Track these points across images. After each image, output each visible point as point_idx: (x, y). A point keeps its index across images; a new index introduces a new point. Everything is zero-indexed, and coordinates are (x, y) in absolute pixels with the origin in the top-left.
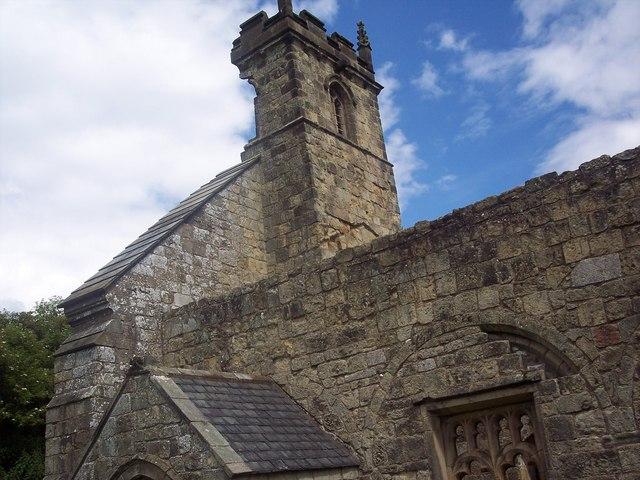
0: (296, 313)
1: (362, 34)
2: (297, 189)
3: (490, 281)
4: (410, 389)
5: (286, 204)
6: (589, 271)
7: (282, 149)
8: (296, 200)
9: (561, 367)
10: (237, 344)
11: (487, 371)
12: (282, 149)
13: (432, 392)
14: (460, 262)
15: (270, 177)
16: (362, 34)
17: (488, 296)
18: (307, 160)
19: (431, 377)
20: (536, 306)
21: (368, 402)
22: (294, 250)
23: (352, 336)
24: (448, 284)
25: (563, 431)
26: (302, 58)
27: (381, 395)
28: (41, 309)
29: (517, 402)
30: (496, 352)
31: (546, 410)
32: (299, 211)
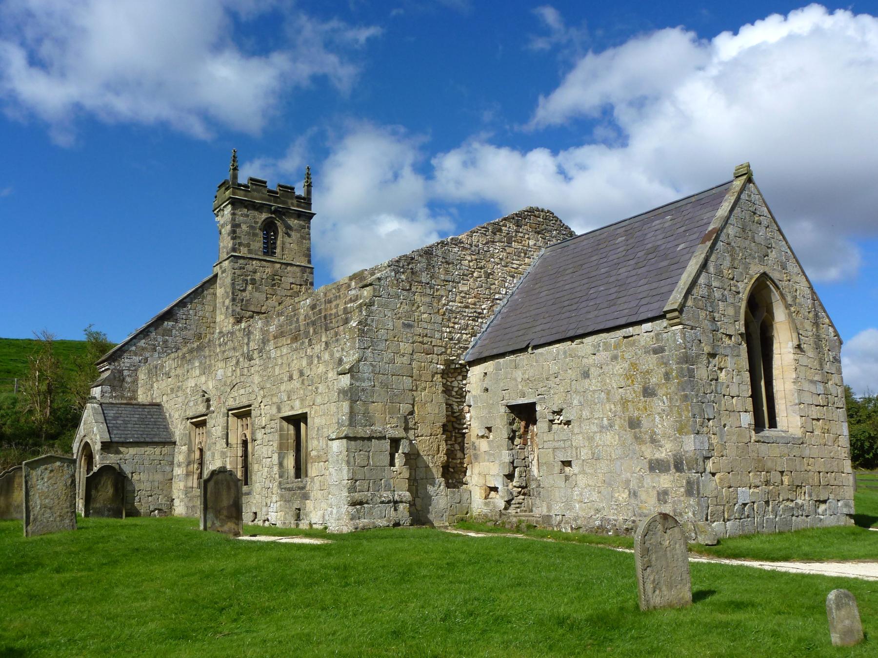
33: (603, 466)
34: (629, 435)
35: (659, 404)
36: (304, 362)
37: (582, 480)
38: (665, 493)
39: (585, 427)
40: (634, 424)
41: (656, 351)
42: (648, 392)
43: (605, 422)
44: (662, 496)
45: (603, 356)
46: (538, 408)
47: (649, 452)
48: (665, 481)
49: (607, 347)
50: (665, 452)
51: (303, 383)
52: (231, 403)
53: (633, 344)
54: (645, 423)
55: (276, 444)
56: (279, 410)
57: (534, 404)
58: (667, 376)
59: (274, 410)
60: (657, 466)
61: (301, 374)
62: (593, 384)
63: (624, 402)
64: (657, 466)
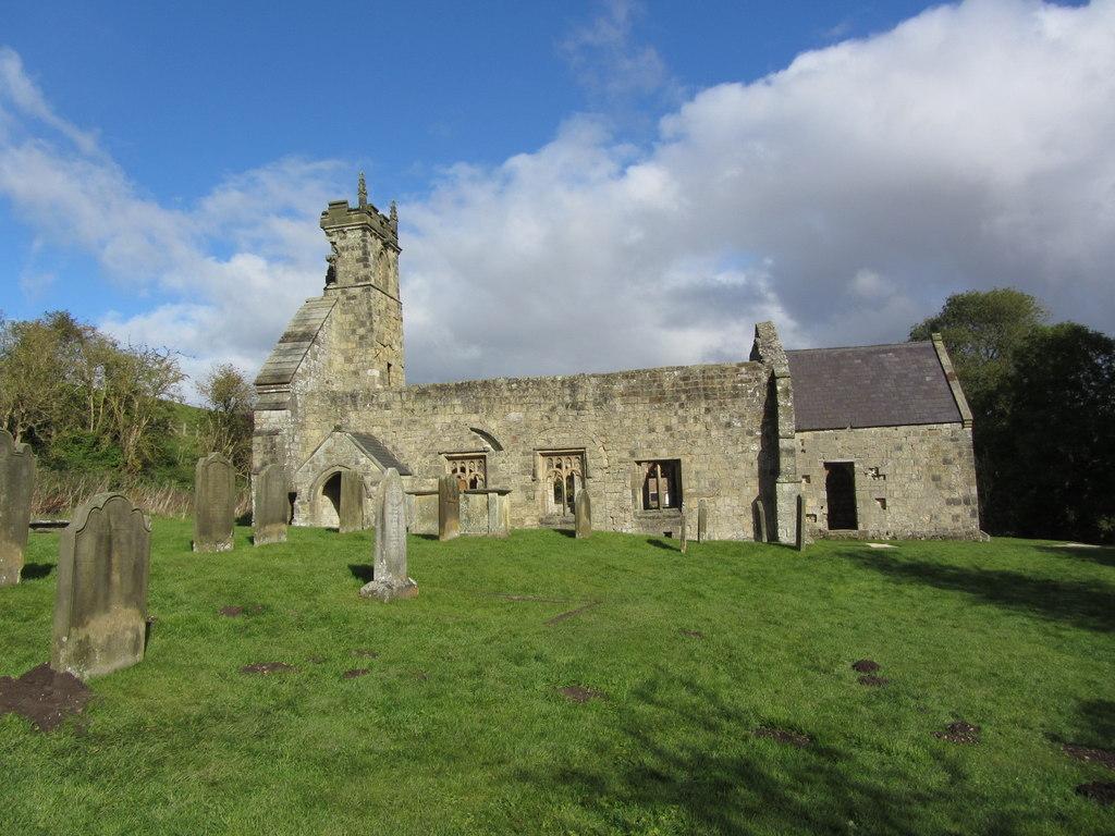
4: (439, 447)
5: (354, 331)
8: (361, 331)
9: (498, 447)
10: (352, 415)
11: (471, 444)
12: (354, 297)
13: (447, 449)
17: (475, 417)
21: (419, 450)
22: (356, 359)
23: (414, 422)
24: (459, 410)
26: (370, 239)
27: (425, 448)
30: (475, 438)
32: (362, 338)
33: (912, 502)
34: (932, 485)
35: (955, 469)
36: (674, 421)
37: (894, 510)
38: (958, 516)
39: (898, 479)
40: (936, 479)
41: (952, 440)
42: (946, 462)
43: (914, 476)
44: (956, 518)
45: (912, 439)
46: (856, 466)
47: (947, 495)
48: (957, 510)
49: (916, 434)
50: (958, 494)
51: (672, 435)
52: (540, 443)
53: (937, 434)
54: (945, 479)
55: (629, 483)
56: (633, 454)
57: (852, 464)
58: (960, 454)
59: (626, 455)
60: (951, 502)
61: (668, 428)
62: (906, 453)
63: (929, 467)
64: (951, 502)
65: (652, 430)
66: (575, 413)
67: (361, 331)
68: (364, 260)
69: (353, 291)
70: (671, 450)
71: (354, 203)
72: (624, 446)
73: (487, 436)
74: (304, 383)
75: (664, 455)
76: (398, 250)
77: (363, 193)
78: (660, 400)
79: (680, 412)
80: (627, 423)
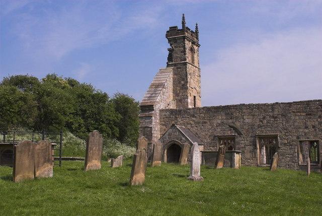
0: (193, 116)
1: (197, 27)
2: (183, 80)
3: (231, 119)
5: (180, 83)
6: (247, 121)
7: (180, 68)
8: (183, 82)
9: (240, 134)
11: (228, 133)
14: (227, 114)
15: (175, 74)
16: (197, 27)
17: (230, 121)
18: (186, 73)
19: (219, 132)
20: (238, 124)
22: (181, 94)
23: (205, 123)
25: (239, 143)
28: (52, 79)
29: (233, 138)
30: (231, 130)
31: (237, 140)
32: (183, 85)
36: (317, 123)
52: (258, 133)
56: (298, 138)
59: (295, 138)
65: (306, 128)
66: (273, 119)
67: (183, 82)
68: (184, 52)
69: (179, 66)
70: (315, 136)
71: (180, 27)
72: (295, 134)
73: (235, 129)
74: (159, 105)
75: (312, 138)
76: (198, 46)
77: (183, 23)
78: (310, 114)
79: (319, 120)
80: (296, 124)
